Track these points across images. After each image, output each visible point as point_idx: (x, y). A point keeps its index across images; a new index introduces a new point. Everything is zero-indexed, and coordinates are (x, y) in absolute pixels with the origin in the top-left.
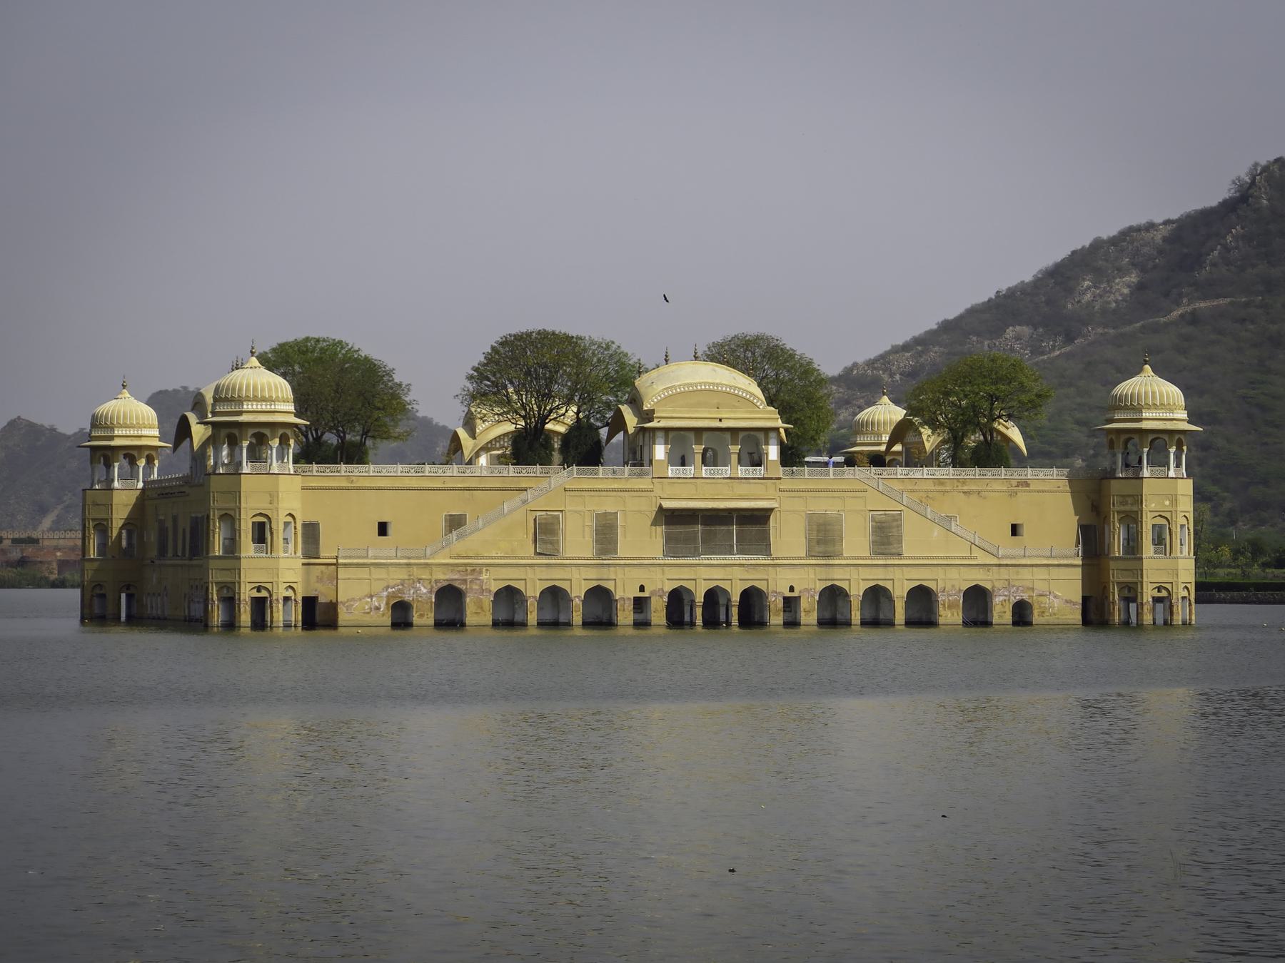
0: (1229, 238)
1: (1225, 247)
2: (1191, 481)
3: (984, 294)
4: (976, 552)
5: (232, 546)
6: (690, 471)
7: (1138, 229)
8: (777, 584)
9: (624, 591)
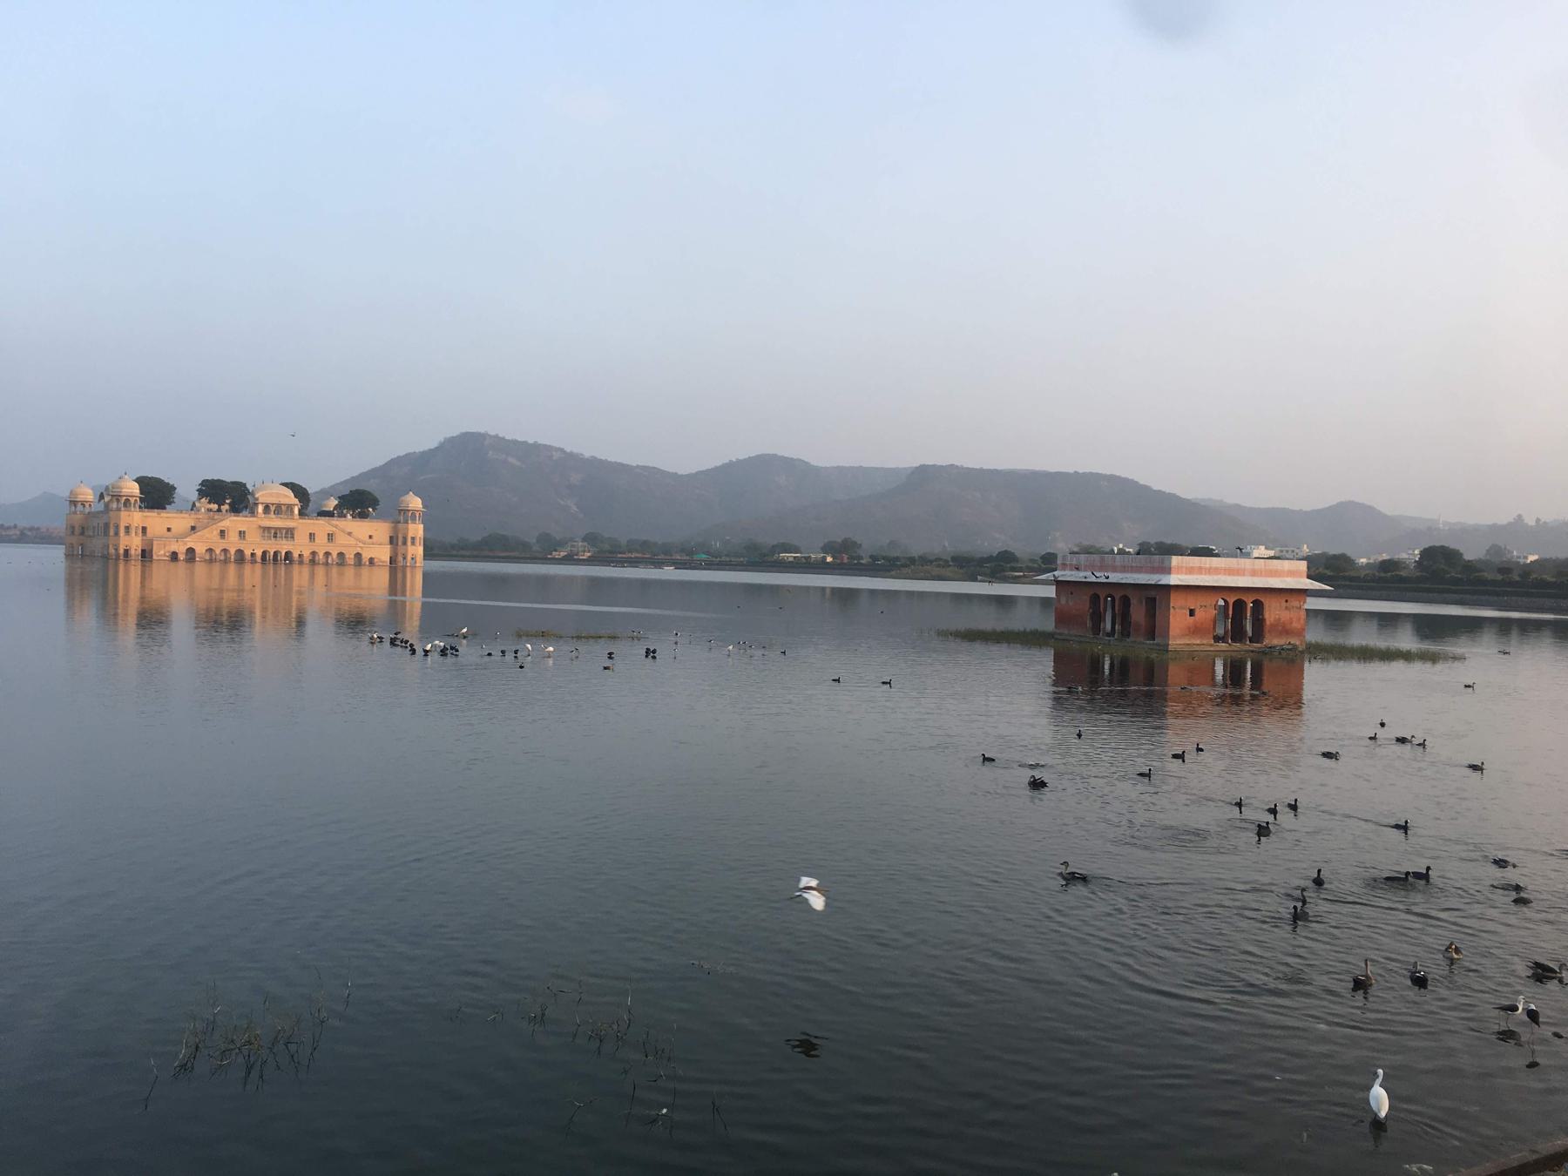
5: (117, 534)
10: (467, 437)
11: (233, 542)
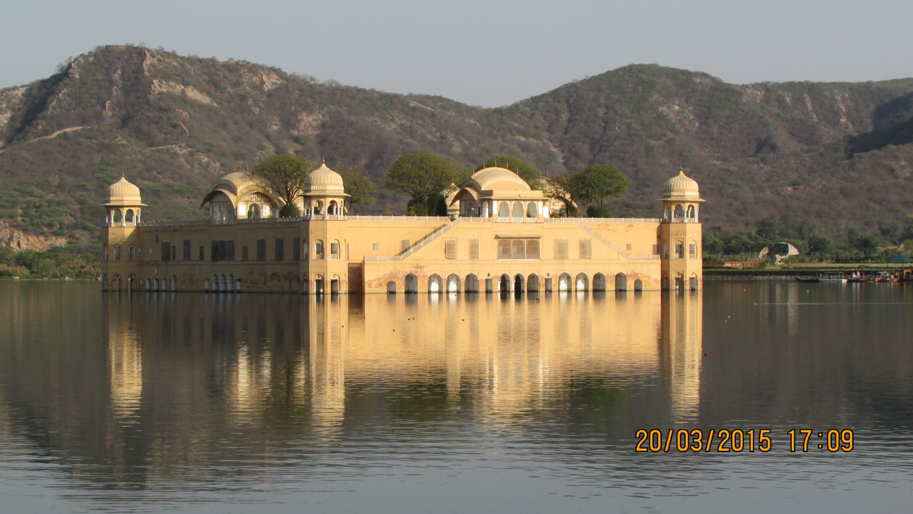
0: (61, 95)
1: (59, 100)
2: (700, 225)
4: (620, 257)
6: (507, 219)
7: (9, 90)
8: (542, 273)
9: (482, 277)
10: (106, 58)
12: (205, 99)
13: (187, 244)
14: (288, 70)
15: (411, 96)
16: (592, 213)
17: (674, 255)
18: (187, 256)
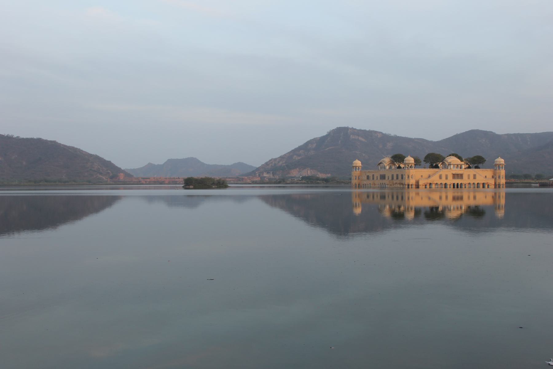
3: (297, 146)
9: (448, 183)
11: (444, 181)
12: (363, 140)
13: (373, 175)
14: (384, 132)
15: (415, 138)
16: (477, 167)
17: (497, 178)
18: (373, 179)
